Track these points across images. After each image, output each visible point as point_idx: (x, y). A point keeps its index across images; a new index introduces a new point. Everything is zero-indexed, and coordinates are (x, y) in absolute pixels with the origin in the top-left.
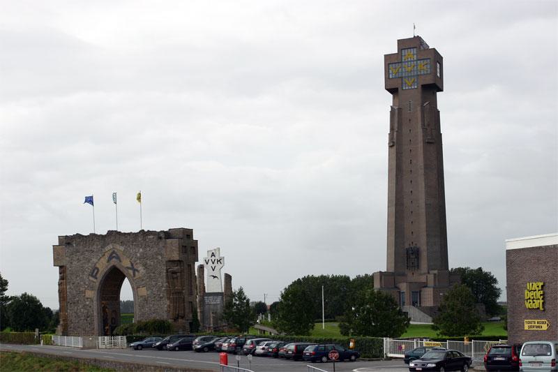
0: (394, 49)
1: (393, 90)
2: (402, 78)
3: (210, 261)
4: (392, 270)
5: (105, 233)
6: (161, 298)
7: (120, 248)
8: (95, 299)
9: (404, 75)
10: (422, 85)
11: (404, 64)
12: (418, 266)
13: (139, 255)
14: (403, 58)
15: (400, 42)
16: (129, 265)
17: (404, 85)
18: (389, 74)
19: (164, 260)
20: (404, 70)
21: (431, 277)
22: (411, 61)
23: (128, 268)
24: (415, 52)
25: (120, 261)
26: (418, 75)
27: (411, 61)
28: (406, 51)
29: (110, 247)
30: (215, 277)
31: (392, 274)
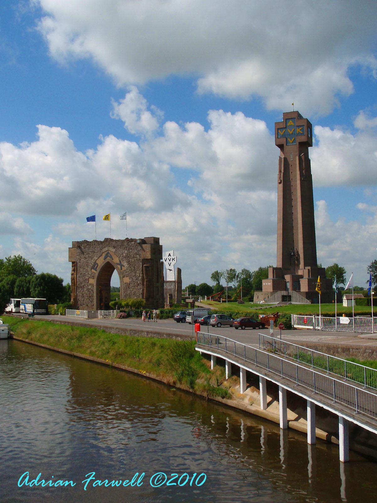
1: (281, 147)
3: (168, 259)
4: (281, 266)
5: (102, 240)
6: (138, 284)
7: (112, 250)
8: (95, 284)
10: (299, 143)
13: (124, 255)
16: (118, 262)
19: (141, 259)
21: (306, 271)
23: (118, 264)
25: (113, 259)
29: (106, 249)
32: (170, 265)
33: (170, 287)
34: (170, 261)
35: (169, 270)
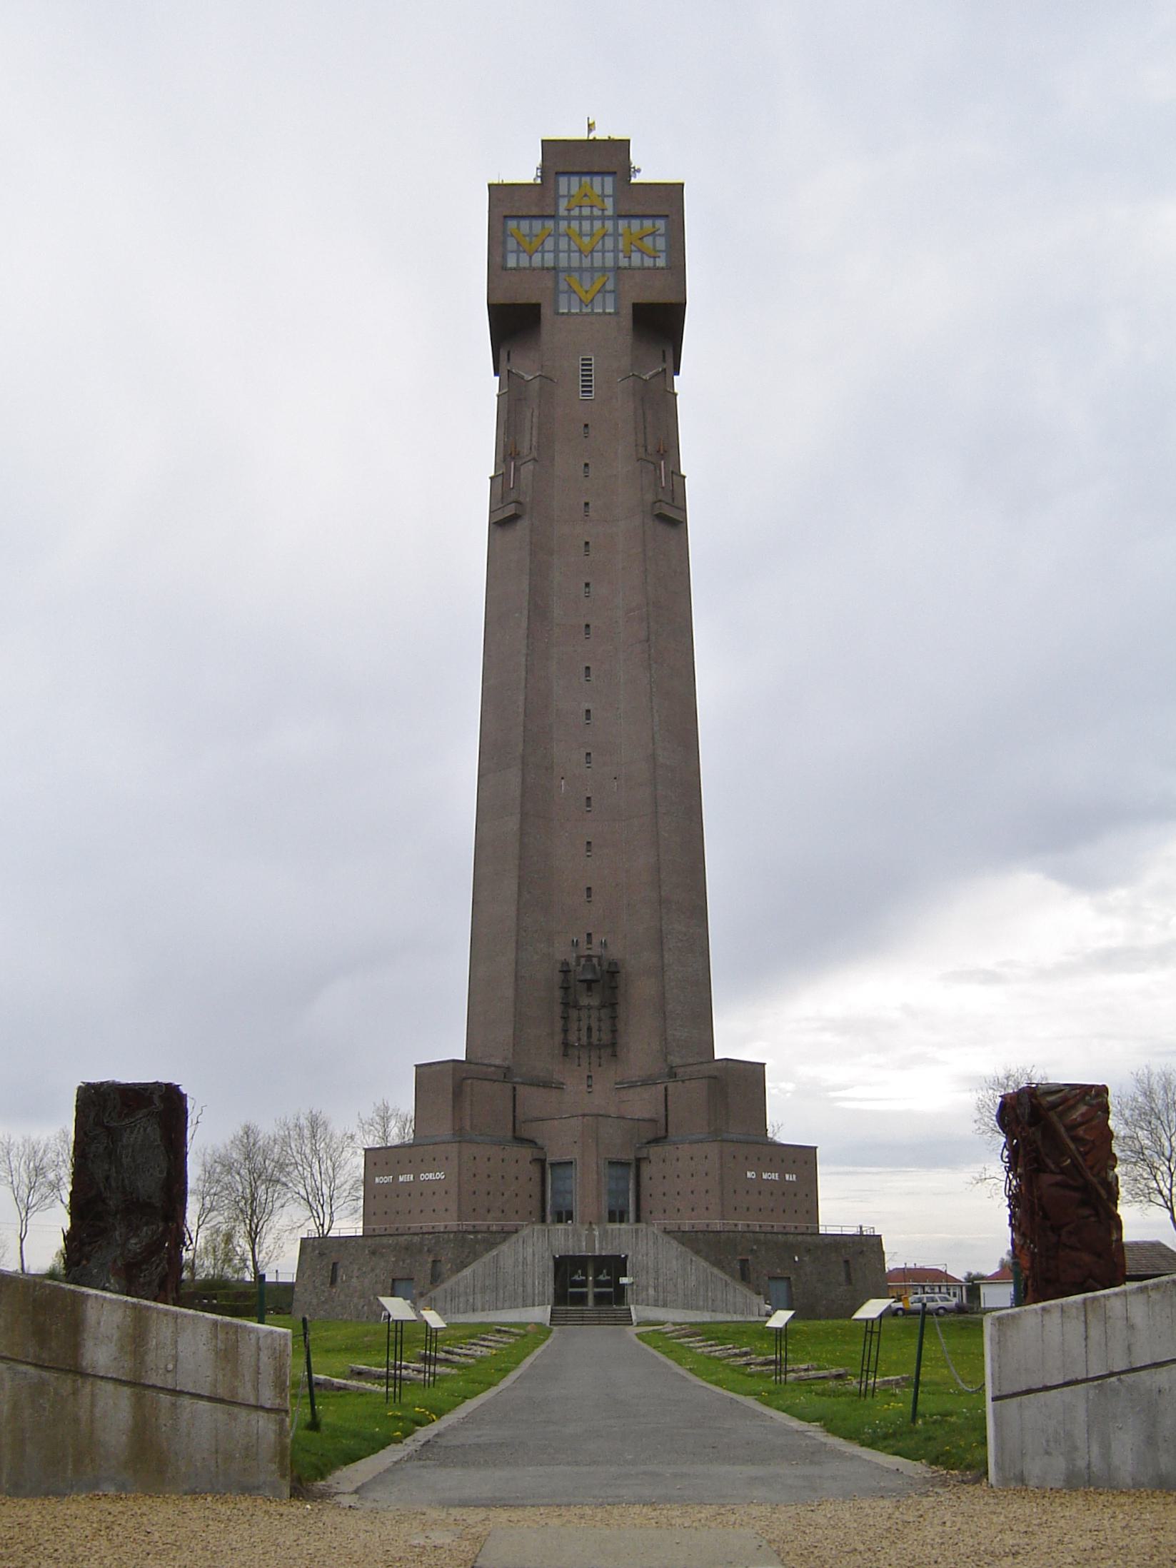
0: (525, 170)
9: (563, 263)
10: (636, 307)
11: (563, 225)
12: (612, 1048)
14: (563, 204)
15: (549, 147)
17: (563, 299)
20: (563, 244)
22: (591, 218)
24: (609, 190)
26: (618, 269)
27: (591, 218)
28: (575, 180)
31: (506, 1074)
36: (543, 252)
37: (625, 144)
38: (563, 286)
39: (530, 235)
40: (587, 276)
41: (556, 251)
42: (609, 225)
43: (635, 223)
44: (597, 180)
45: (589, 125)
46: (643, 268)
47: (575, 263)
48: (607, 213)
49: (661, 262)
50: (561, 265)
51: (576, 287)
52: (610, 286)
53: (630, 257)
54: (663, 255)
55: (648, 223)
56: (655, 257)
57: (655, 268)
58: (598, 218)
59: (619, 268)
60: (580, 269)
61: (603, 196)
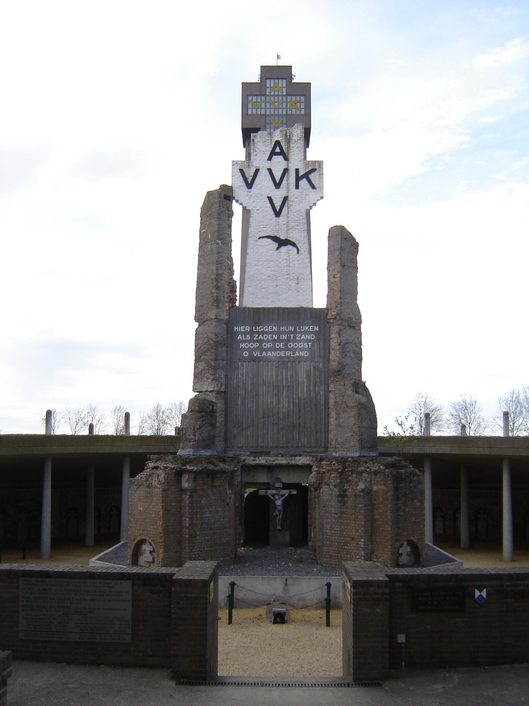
0: (255, 77)
2: (265, 115)
3: (264, 176)
9: (268, 113)
11: (268, 98)
15: (264, 69)
18: (248, 109)
20: (268, 106)
24: (284, 85)
26: (287, 115)
27: (278, 96)
28: (272, 81)
30: (282, 243)
32: (278, 214)
33: (287, 349)
34: (278, 185)
35: (275, 239)
36: (261, 108)
37: (290, 67)
38: (268, 121)
39: (257, 102)
40: (276, 117)
41: (266, 108)
42: (284, 98)
43: (294, 98)
44: (280, 81)
45: (278, 56)
46: (296, 115)
47: (272, 113)
48: (283, 94)
49: (303, 112)
50: (267, 114)
51: (272, 122)
52: (284, 122)
53: (291, 111)
54: (303, 110)
55: (298, 98)
56: (300, 111)
57: (300, 115)
58: (280, 96)
59: (288, 115)
60: (274, 115)
61: (282, 87)
